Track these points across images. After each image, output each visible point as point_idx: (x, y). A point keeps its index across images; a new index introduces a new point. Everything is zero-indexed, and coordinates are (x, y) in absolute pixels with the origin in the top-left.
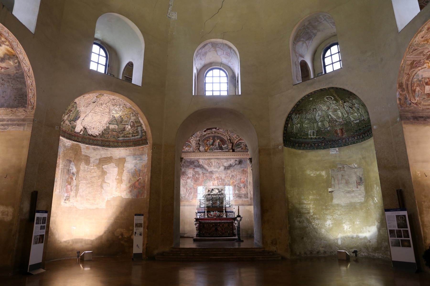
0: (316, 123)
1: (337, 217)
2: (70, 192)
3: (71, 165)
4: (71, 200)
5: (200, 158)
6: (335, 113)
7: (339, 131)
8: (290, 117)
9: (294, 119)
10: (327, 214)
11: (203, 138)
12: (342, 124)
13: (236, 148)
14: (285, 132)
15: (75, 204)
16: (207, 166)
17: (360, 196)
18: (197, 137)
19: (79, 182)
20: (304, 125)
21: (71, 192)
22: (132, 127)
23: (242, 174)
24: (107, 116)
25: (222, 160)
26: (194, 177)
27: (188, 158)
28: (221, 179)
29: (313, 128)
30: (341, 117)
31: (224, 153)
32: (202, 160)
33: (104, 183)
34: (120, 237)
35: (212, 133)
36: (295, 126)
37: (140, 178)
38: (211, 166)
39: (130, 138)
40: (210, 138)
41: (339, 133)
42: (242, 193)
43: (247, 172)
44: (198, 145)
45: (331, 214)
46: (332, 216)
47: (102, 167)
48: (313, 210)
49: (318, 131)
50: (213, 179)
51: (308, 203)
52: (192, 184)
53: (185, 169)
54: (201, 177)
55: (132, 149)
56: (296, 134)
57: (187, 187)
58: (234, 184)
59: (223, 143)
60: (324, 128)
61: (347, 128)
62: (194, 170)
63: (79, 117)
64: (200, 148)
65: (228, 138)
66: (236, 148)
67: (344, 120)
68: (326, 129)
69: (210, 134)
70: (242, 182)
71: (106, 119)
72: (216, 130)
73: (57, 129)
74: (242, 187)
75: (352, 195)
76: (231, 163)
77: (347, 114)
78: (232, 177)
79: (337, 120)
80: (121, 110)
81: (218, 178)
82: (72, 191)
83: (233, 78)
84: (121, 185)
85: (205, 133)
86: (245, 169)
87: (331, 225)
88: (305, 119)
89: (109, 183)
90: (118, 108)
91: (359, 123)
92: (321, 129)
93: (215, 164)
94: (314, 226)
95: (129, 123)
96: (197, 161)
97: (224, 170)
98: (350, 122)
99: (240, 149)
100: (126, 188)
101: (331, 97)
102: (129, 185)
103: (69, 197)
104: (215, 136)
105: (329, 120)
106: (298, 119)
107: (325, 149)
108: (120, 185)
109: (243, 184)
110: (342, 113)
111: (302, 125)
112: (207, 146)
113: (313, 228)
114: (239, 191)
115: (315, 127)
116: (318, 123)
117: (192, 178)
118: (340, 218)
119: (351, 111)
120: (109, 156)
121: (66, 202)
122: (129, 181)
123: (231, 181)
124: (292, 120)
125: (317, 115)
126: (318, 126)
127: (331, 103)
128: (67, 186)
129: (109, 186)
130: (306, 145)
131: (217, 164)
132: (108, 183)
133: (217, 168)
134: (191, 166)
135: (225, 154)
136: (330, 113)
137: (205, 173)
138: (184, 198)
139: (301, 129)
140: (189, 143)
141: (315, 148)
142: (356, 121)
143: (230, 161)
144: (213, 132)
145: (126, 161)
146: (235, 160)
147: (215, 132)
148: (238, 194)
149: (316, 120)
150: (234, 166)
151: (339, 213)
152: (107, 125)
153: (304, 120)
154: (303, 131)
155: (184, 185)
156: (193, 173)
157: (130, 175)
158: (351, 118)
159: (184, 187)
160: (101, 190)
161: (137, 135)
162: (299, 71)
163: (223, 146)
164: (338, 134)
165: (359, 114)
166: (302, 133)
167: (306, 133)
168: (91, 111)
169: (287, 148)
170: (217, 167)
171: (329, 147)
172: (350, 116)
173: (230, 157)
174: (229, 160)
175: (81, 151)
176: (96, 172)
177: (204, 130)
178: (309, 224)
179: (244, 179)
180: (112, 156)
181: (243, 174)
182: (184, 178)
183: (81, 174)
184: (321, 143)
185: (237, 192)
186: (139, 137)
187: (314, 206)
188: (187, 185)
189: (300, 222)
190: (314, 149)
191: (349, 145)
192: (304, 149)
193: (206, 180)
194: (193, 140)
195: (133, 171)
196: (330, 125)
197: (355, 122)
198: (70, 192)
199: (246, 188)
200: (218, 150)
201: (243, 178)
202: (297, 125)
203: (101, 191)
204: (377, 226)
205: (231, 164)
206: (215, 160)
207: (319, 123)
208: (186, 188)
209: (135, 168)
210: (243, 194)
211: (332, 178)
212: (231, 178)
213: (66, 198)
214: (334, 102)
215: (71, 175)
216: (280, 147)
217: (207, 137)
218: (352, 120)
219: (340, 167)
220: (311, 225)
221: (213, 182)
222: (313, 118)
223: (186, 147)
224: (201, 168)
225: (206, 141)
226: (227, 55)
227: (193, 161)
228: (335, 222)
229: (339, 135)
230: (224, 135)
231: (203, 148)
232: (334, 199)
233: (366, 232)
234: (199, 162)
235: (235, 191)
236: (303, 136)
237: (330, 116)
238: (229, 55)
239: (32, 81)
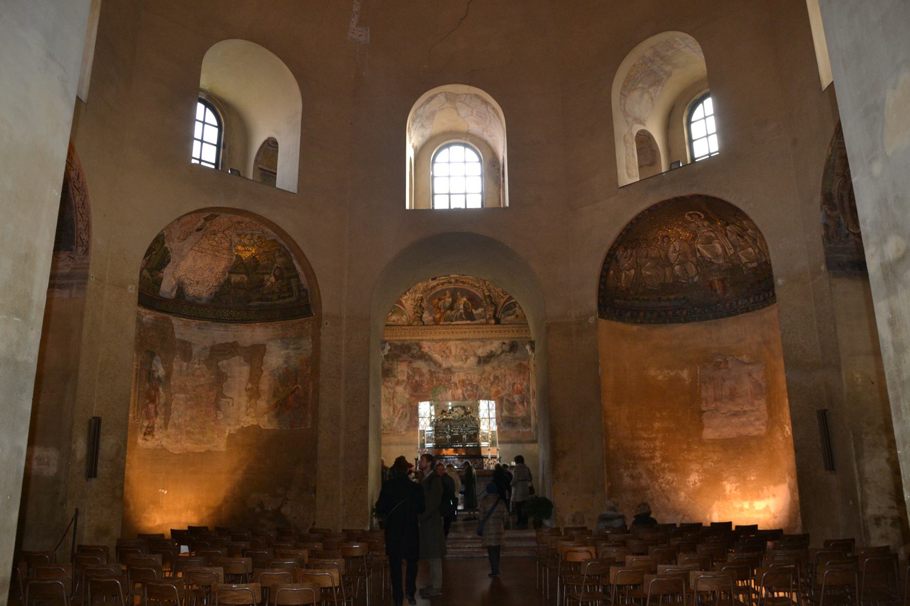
1: (711, 466)
2: (154, 418)
3: (155, 362)
4: (158, 434)
5: (424, 338)
7: (718, 284)
8: (613, 255)
9: (622, 259)
10: (690, 461)
12: (723, 268)
13: (503, 315)
14: (602, 287)
15: (164, 443)
16: (440, 357)
17: (757, 423)
18: (416, 291)
19: (171, 396)
21: (156, 417)
22: (277, 278)
23: (517, 373)
24: (224, 256)
25: (473, 343)
26: (410, 381)
27: (397, 338)
28: (471, 384)
30: (721, 255)
31: (477, 326)
32: (428, 343)
33: (222, 398)
34: (258, 510)
35: (450, 283)
36: (623, 275)
37: (296, 386)
38: (447, 357)
39: (273, 302)
40: (445, 295)
41: (717, 287)
42: (516, 414)
43: (528, 369)
44: (419, 309)
45: (698, 461)
46: (702, 464)
47: (217, 365)
48: (661, 452)
50: (453, 385)
51: (651, 436)
52: (407, 396)
53: (390, 362)
54: (426, 381)
55: (278, 325)
56: (626, 290)
57: (395, 402)
58: (499, 396)
60: (686, 278)
62: (411, 364)
63: (169, 261)
64: (424, 316)
65: (486, 294)
66: (503, 315)
67: (727, 262)
69: (445, 285)
70: (516, 392)
71: (222, 264)
73: (131, 291)
74: (518, 402)
75: (741, 419)
76: (493, 349)
77: (733, 250)
78: (494, 381)
79: (713, 260)
80: (255, 243)
81: (463, 383)
82: (158, 416)
83: (494, 166)
84: (258, 402)
86: (523, 362)
87: (699, 484)
89: (231, 398)
90: (248, 239)
91: (757, 269)
93: (458, 351)
94: (664, 485)
95: (272, 270)
96: (418, 345)
97: (477, 366)
98: (739, 265)
99: (513, 317)
100: (268, 408)
101: (699, 213)
102: (273, 403)
103: (152, 427)
104: (455, 290)
105: (697, 259)
106: (630, 259)
107: (689, 322)
108: (256, 403)
109: (520, 395)
110: (723, 247)
112: (438, 311)
113: (660, 490)
114: (510, 410)
115: (668, 275)
116: (674, 267)
117: (405, 384)
118: (716, 468)
120: (231, 341)
121: (147, 438)
122: (275, 393)
123: (492, 389)
124: (617, 261)
125: (671, 249)
126: (674, 273)
127: (700, 225)
128: (147, 405)
129: (232, 405)
131: (462, 351)
132: (229, 397)
133: (462, 360)
134: (405, 356)
137: (434, 372)
138: (389, 428)
139: (637, 279)
140: (399, 306)
141: (668, 321)
142: (750, 263)
143: (491, 344)
145: (267, 351)
146: (501, 342)
147: (457, 281)
148: (508, 417)
150: (498, 356)
151: (715, 458)
152: (225, 275)
154: (642, 284)
155: (389, 398)
156: (408, 373)
157: (275, 380)
158: (743, 257)
159: (389, 403)
160: (216, 413)
161: (290, 296)
162: (633, 155)
163: (473, 310)
164: (716, 290)
165: (757, 251)
167: (649, 288)
168: (194, 248)
169: (607, 321)
170: (461, 357)
171: (697, 318)
173: (491, 336)
174: (489, 342)
175: (173, 333)
176: (204, 376)
178: (651, 482)
179: (523, 383)
180: (237, 340)
181: (520, 372)
182: (389, 384)
183: (175, 381)
184: (679, 309)
185: (505, 413)
186: (293, 299)
187: (664, 444)
188: (395, 399)
189: (632, 477)
190: (665, 322)
191: (738, 314)
193: (437, 387)
194: (409, 297)
195: (281, 371)
196: (698, 272)
197: (750, 265)
198: (154, 418)
199: (525, 404)
200: (463, 320)
201: (519, 382)
203: (217, 416)
204: (789, 484)
205: (492, 352)
206: (457, 342)
207: (676, 266)
208: (392, 405)
209: (285, 366)
210: (519, 418)
211: (703, 385)
212: (492, 384)
213: (147, 431)
214: (706, 223)
215: (154, 382)
216: (591, 320)
217: (438, 292)
219: (718, 362)
220: (657, 484)
221: (453, 391)
222: (662, 256)
223: (393, 313)
224: (426, 360)
225: (436, 300)
226: (480, 117)
227: (408, 344)
228: (708, 476)
229: (719, 292)
230: (476, 287)
231: (430, 316)
232: (705, 429)
233: (768, 497)
234: (421, 348)
235: (502, 411)
237: (699, 251)
238: (484, 117)
239: (85, 199)
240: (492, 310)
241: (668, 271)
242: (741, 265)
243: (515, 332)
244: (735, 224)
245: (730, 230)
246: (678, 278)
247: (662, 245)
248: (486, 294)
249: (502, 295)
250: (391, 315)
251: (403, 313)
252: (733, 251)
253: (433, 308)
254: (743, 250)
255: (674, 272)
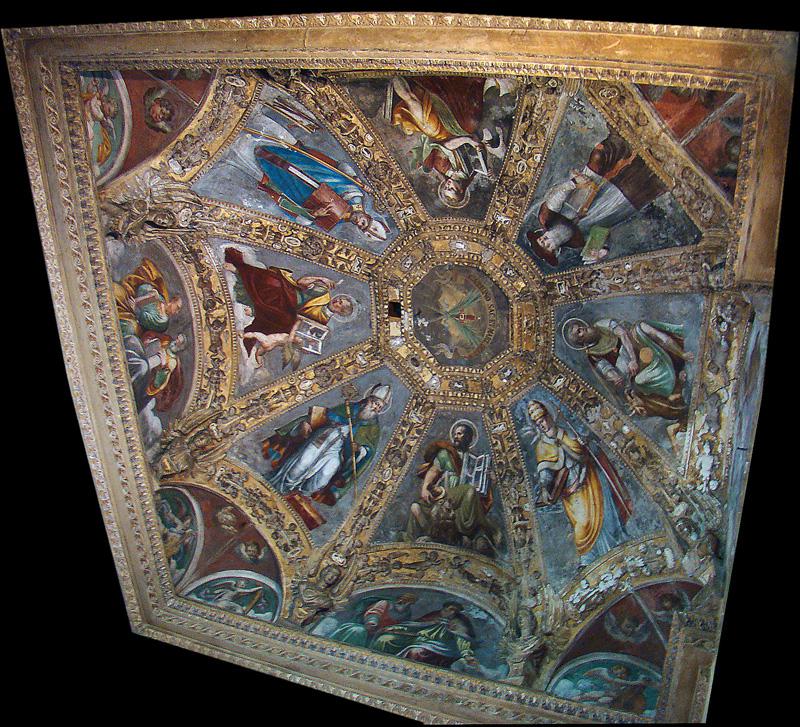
11: (166, 250)
35: (210, 306)
40: (173, 299)
59: (163, 399)
64: (111, 243)
69: (199, 291)
72: (241, 327)
85: (213, 256)
99: (162, 527)
135: (126, 456)
144: (217, 313)
163: (151, 404)
177: (242, 249)
223: (102, 122)
240: (177, 465)
243: (143, 568)
248: (213, 427)
249: (218, 474)
250: (95, 118)
251: (107, 164)
253: (134, 268)
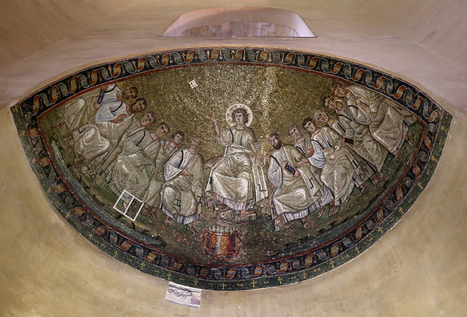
0: (160, 184)
6: (231, 180)
12: (237, 219)
20: (119, 161)
29: (143, 188)
30: (245, 197)
36: (92, 131)
49: (153, 210)
61: (255, 234)
68: (182, 218)
77: (266, 192)
79: (228, 203)
88: (134, 142)
91: (304, 221)
92: (165, 208)
98: (270, 216)
105: (203, 197)
107: (153, 274)
110: (252, 186)
111: (114, 153)
116: (166, 186)
119: (285, 182)
125: (176, 159)
127: (236, 139)
130: (89, 222)
136: (214, 176)
141: (116, 253)
142: (293, 213)
149: (163, 174)
153: (130, 145)
158: (280, 204)
166: (98, 175)
167: (112, 188)
169: (19, 141)
171: (169, 275)
172: (274, 199)
184: (145, 248)
190: (109, 251)
192: (75, 227)
197: (290, 217)
202: (101, 135)
207: (168, 188)
214: (247, 137)
218: (279, 213)
222: (157, 161)
236: (97, 188)
237: (211, 183)
241: (154, 186)
242: (273, 218)
244: (293, 145)
245: (278, 159)
246: (162, 205)
247: (167, 143)
252: (267, 196)
254: (285, 194)
255: (161, 193)
